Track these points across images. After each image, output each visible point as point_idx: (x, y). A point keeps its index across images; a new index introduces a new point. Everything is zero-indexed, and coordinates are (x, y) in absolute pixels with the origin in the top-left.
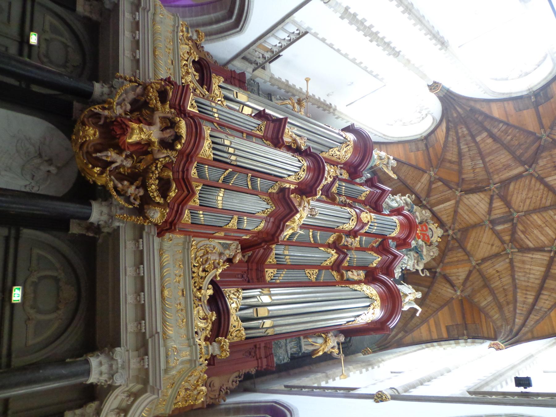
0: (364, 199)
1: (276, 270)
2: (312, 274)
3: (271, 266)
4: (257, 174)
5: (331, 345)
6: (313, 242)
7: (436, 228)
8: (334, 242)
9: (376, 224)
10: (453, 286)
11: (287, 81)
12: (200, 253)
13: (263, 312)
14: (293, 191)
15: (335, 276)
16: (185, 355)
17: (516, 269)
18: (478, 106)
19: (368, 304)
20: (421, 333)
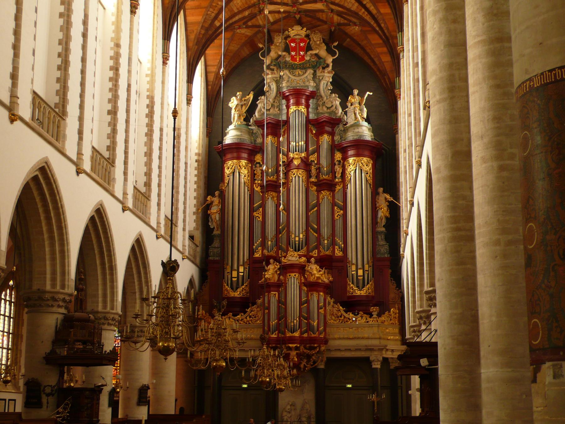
0: (276, 138)
1: (336, 247)
2: (338, 213)
3: (334, 251)
4: (301, 304)
5: (383, 199)
6: (316, 209)
7: (293, 30)
8: (315, 185)
9: (300, 143)
10: (349, 25)
11: (194, 213)
12: (333, 318)
13: (360, 272)
14: (304, 277)
15: (339, 188)
16: (375, 329)
17: (342, 3)
18: (192, 37)
19: (360, 171)
20: (388, 62)
